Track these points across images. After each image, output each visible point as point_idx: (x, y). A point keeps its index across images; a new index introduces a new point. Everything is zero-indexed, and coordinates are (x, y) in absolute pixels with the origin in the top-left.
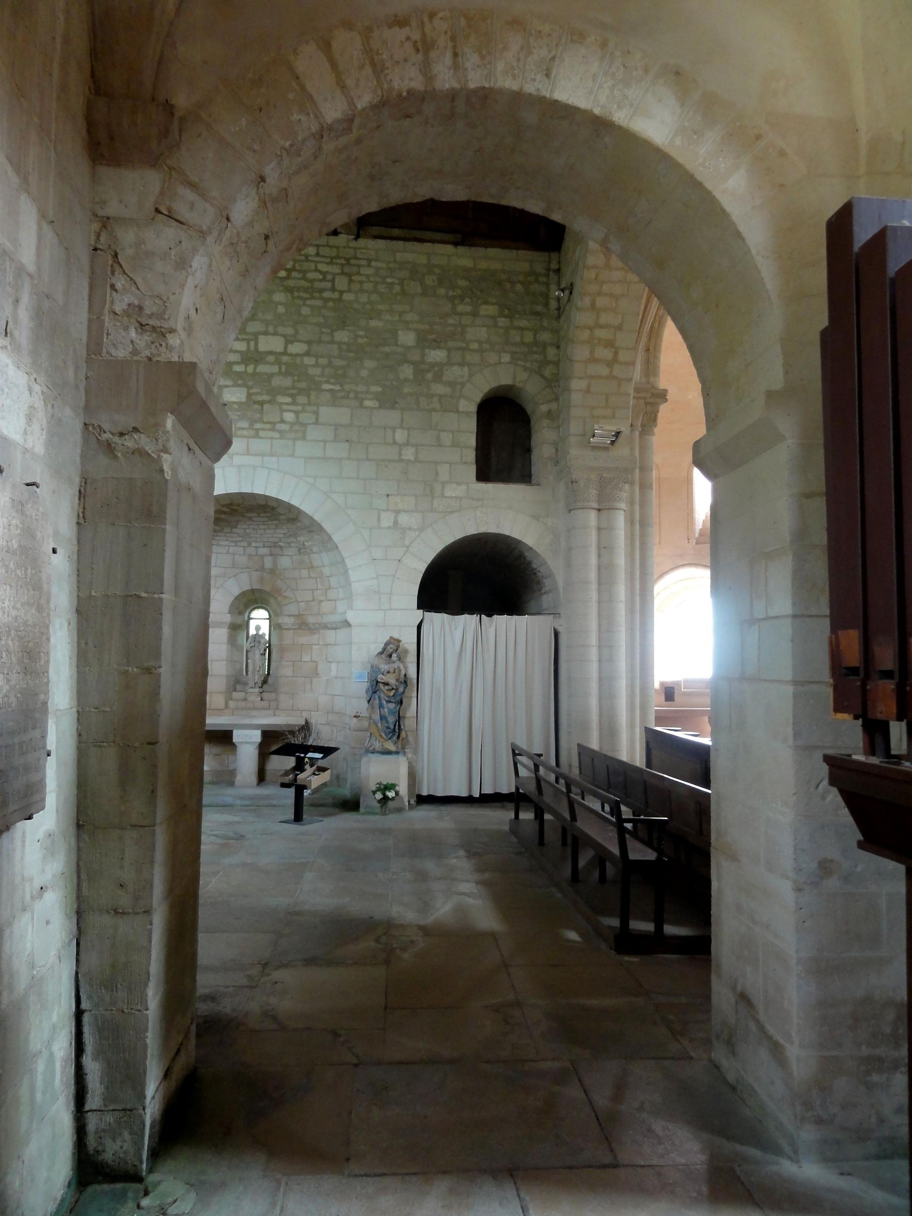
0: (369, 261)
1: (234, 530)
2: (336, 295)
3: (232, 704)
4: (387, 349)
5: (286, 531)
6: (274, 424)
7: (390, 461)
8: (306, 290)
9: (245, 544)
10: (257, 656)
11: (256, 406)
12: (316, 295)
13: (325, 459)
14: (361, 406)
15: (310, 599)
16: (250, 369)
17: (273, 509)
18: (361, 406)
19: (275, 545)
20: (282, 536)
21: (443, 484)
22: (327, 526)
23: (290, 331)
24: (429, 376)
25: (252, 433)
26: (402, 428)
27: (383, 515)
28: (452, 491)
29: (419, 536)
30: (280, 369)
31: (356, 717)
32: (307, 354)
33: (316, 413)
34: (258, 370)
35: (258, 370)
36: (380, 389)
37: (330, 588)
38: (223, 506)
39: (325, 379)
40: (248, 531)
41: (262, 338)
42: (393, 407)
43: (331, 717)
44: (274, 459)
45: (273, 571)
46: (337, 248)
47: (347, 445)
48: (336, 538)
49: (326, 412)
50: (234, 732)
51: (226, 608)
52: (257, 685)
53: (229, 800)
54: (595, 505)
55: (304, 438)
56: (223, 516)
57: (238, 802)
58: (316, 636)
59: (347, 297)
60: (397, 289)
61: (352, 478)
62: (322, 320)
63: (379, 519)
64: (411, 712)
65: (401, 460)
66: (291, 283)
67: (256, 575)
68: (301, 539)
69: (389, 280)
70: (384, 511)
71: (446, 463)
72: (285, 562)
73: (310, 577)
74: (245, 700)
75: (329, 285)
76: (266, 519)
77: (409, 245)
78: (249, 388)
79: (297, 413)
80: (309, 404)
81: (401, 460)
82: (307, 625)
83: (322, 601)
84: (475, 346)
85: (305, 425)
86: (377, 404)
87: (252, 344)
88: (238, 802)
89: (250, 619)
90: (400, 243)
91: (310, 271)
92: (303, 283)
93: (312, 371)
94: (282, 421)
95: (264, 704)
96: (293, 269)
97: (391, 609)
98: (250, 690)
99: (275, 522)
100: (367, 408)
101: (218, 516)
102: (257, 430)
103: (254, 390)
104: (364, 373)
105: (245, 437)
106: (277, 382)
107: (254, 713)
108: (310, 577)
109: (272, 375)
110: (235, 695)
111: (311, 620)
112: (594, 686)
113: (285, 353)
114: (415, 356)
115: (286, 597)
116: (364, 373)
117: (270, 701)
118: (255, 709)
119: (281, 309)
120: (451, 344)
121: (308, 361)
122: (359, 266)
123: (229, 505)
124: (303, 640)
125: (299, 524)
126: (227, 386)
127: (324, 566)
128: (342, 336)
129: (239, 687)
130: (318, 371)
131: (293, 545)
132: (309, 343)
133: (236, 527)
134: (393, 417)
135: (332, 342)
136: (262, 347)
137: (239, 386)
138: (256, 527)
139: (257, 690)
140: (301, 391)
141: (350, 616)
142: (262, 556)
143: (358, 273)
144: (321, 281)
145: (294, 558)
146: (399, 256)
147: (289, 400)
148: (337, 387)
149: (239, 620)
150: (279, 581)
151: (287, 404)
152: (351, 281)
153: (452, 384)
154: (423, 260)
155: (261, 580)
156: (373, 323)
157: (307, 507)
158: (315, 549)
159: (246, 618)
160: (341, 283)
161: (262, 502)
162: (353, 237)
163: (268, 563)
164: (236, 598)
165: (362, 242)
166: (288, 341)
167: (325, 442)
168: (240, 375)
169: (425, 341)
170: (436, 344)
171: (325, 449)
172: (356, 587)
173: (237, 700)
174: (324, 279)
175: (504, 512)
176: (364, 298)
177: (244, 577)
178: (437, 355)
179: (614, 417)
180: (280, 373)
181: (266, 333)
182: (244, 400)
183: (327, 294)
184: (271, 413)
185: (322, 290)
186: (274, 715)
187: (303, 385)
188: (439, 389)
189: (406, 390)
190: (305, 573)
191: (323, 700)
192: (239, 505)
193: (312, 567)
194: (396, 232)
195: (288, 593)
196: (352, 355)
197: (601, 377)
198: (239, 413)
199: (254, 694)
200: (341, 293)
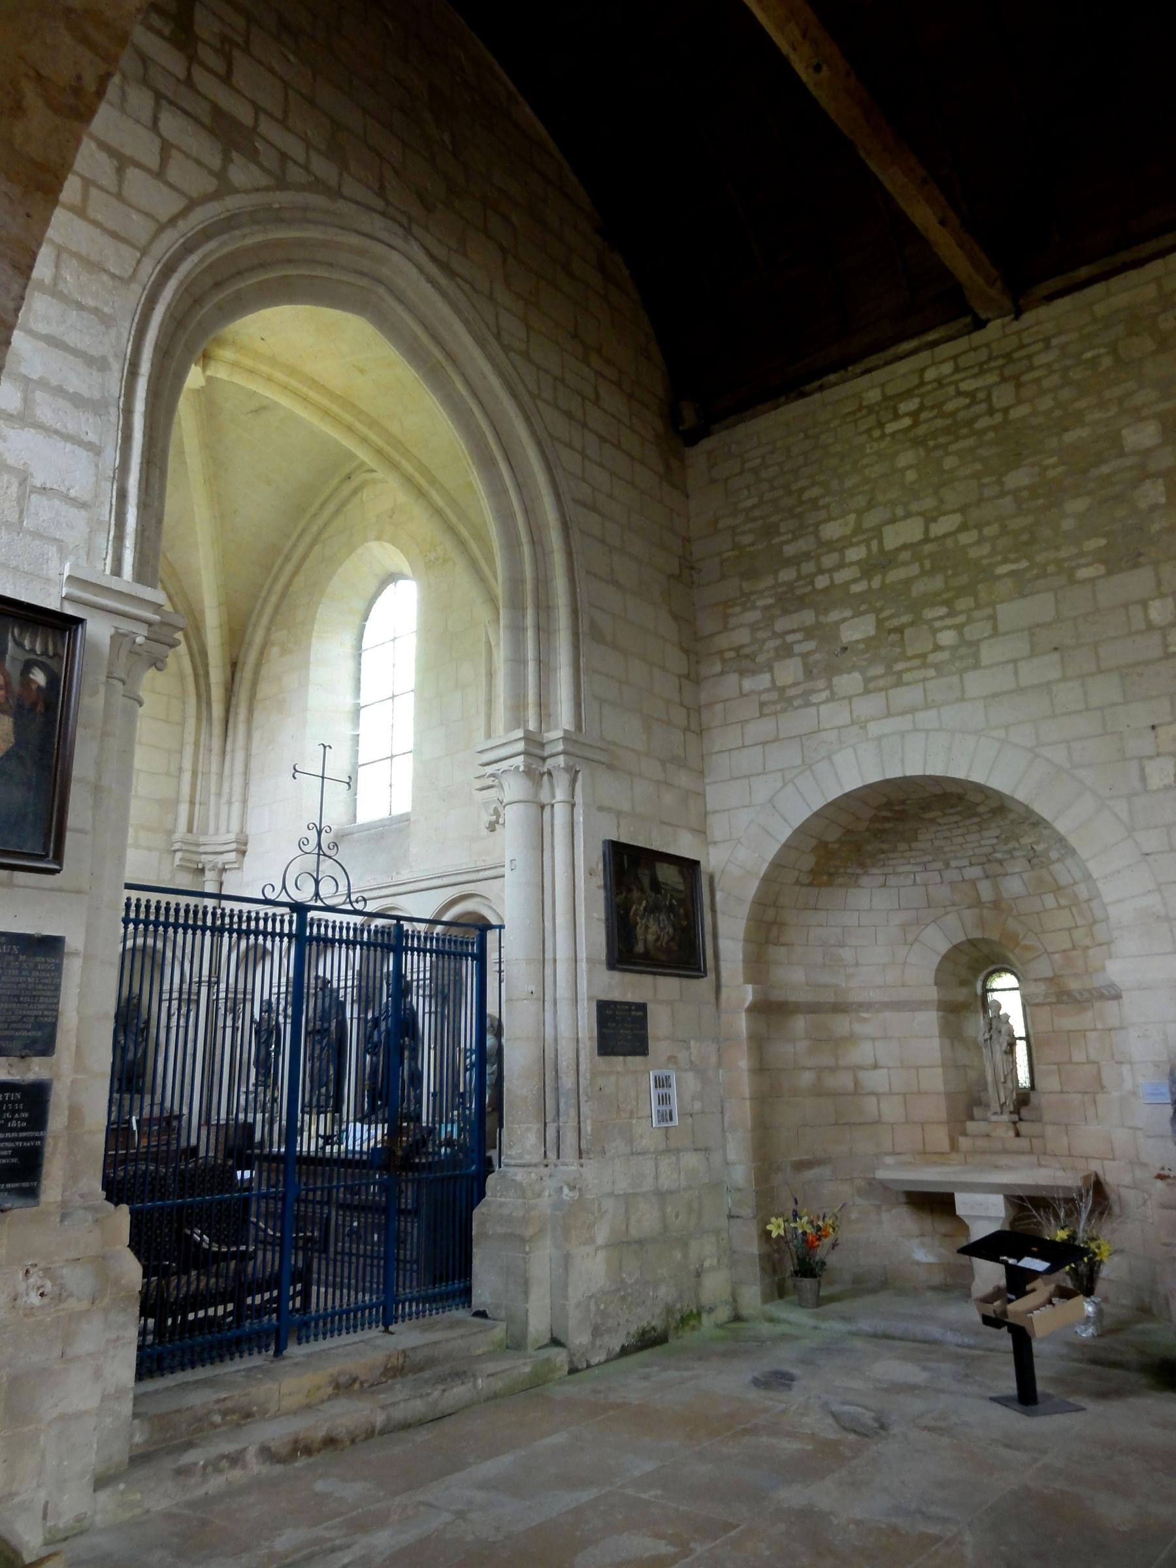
0: (1047, 341)
1: (914, 845)
2: (998, 418)
3: (964, 1143)
4: (1105, 469)
5: (997, 832)
6: (924, 656)
7: (1146, 663)
8: (947, 431)
9: (939, 865)
10: (999, 1056)
11: (894, 637)
12: (964, 431)
13: (1020, 690)
14: (1072, 581)
15: (1070, 946)
16: (876, 583)
17: (961, 798)
18: (1072, 581)
19: (988, 859)
20: (995, 841)
22: (1041, 808)
23: (929, 503)
25: (891, 680)
26: (1162, 596)
27: (1151, 767)
30: (922, 565)
31: (1161, 1177)
32: (963, 528)
33: (993, 618)
34: (888, 581)
35: (888, 581)
36: (1103, 542)
37: (1095, 922)
38: (878, 808)
39: (999, 558)
40: (937, 843)
41: (888, 530)
42: (1136, 566)
43: (1139, 1173)
44: (933, 713)
45: (996, 905)
46: (987, 345)
47: (1056, 656)
48: (1062, 826)
49: (1008, 612)
50: (956, 1195)
51: (930, 977)
52: (1006, 1110)
53: (934, 1331)
55: (977, 666)
56: (887, 825)
57: (950, 1337)
58: (1090, 1014)
59: (1017, 413)
60: (1107, 362)
61: (1075, 712)
62: (978, 466)
63: (1143, 778)
66: (921, 430)
67: (968, 914)
68: (1026, 841)
69: (1089, 355)
70: (1151, 758)
72: (1013, 886)
73: (1060, 907)
74: (988, 1136)
75: (983, 407)
76: (957, 818)
77: (1115, 283)
78: (877, 611)
79: (959, 628)
80: (978, 607)
82: (1069, 993)
83: (1087, 948)
85: (976, 643)
86: (1102, 569)
87: (874, 545)
88: (950, 1337)
89: (986, 991)
90: (1098, 289)
91: (950, 399)
92: (940, 423)
93: (973, 553)
94: (937, 648)
95: (1023, 1143)
96: (922, 408)
98: (994, 1118)
99: (976, 820)
100: (1083, 582)
101: (878, 826)
102: (900, 673)
103: (886, 614)
104: (1068, 524)
105: (881, 690)
106: (917, 589)
107: (1004, 1160)
108: (1060, 907)
109: (908, 582)
110: (971, 1126)
111: (1074, 985)
113: (926, 540)
115: (1026, 948)
117: (1031, 1137)
118: (1006, 1152)
119: (911, 475)
121: (965, 538)
122: (1029, 357)
123: (889, 805)
124: (1068, 1022)
125: (1011, 816)
126: (844, 620)
127: (1075, 883)
128: (1019, 478)
129: (977, 1112)
130: (986, 549)
131: (1017, 854)
132: (963, 510)
133: (916, 840)
134: (1138, 582)
135: (1002, 494)
136: (890, 543)
137: (862, 614)
138: (948, 834)
139: (1006, 1117)
140: (962, 591)
141: (1117, 971)
142: (973, 882)
143: (1031, 368)
144: (968, 406)
145: (1025, 876)
146: (1100, 310)
147: (943, 611)
148: (1024, 564)
149: (961, 995)
150: (1011, 921)
151: (941, 618)
152: (1019, 385)
154: (1151, 291)
155: (982, 923)
156: (1069, 437)
157: (1000, 782)
158: (1054, 855)
159: (979, 991)
160: (1003, 396)
161: (937, 790)
162: (1012, 316)
163: (986, 891)
164: (945, 958)
165: (1028, 317)
166: (929, 519)
167: (1015, 661)
168: (862, 597)
171: (1016, 673)
173: (975, 1136)
174: (974, 402)
176: (1046, 403)
177: (951, 919)
180: (923, 573)
181: (893, 520)
182: (872, 632)
183: (980, 424)
184: (917, 642)
185: (970, 423)
186: (1040, 1165)
187: (964, 579)
189: (1155, 527)
190: (1050, 901)
191: (1120, 1136)
192: (903, 803)
193: (1059, 888)
194: (1084, 272)
195: (1030, 941)
196: (1041, 501)
198: (867, 656)
199: (1000, 1125)
200: (1006, 411)
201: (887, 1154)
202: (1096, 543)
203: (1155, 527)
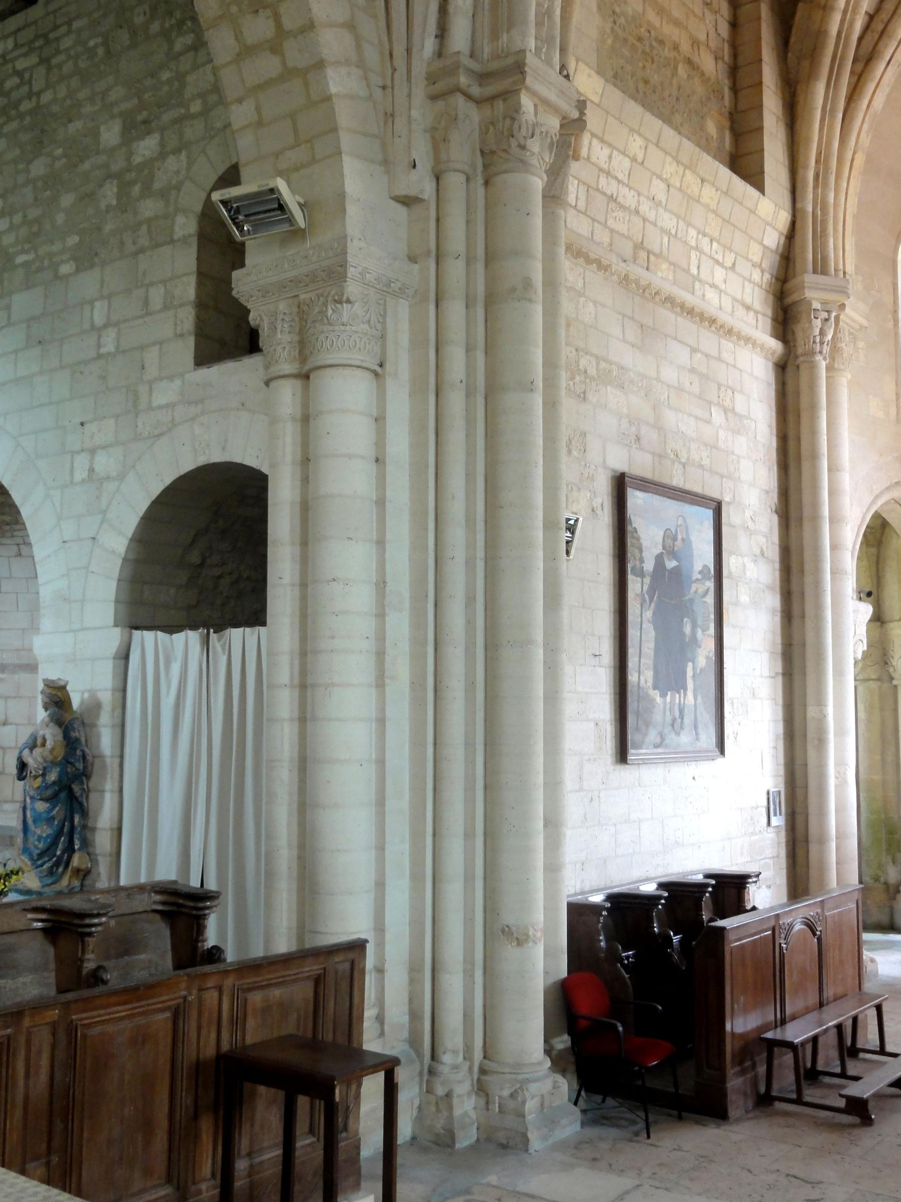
0: (69, 23)
4: (87, 166)
7: (86, 362)
13: (17, 381)
21: (150, 383)
24: (137, 189)
26: (102, 297)
28: (165, 394)
29: (118, 489)
42: (92, 266)
54: (287, 368)
60: (101, 51)
64: (104, 819)
65: (99, 356)
71: (154, 344)
81: (99, 356)
84: (196, 107)
97: (83, 629)
112: (284, 777)
114: (118, 165)
116: (60, 218)
120: (166, 117)
128: (39, 168)
143: (58, 52)
153: (164, 194)
169: (134, 129)
170: (146, 127)
172: (46, 593)
175: (222, 419)
178: (147, 147)
179: (313, 161)
188: (149, 208)
197: (269, 83)
201: (6, 802)
202: (73, 240)
203: (108, 228)
